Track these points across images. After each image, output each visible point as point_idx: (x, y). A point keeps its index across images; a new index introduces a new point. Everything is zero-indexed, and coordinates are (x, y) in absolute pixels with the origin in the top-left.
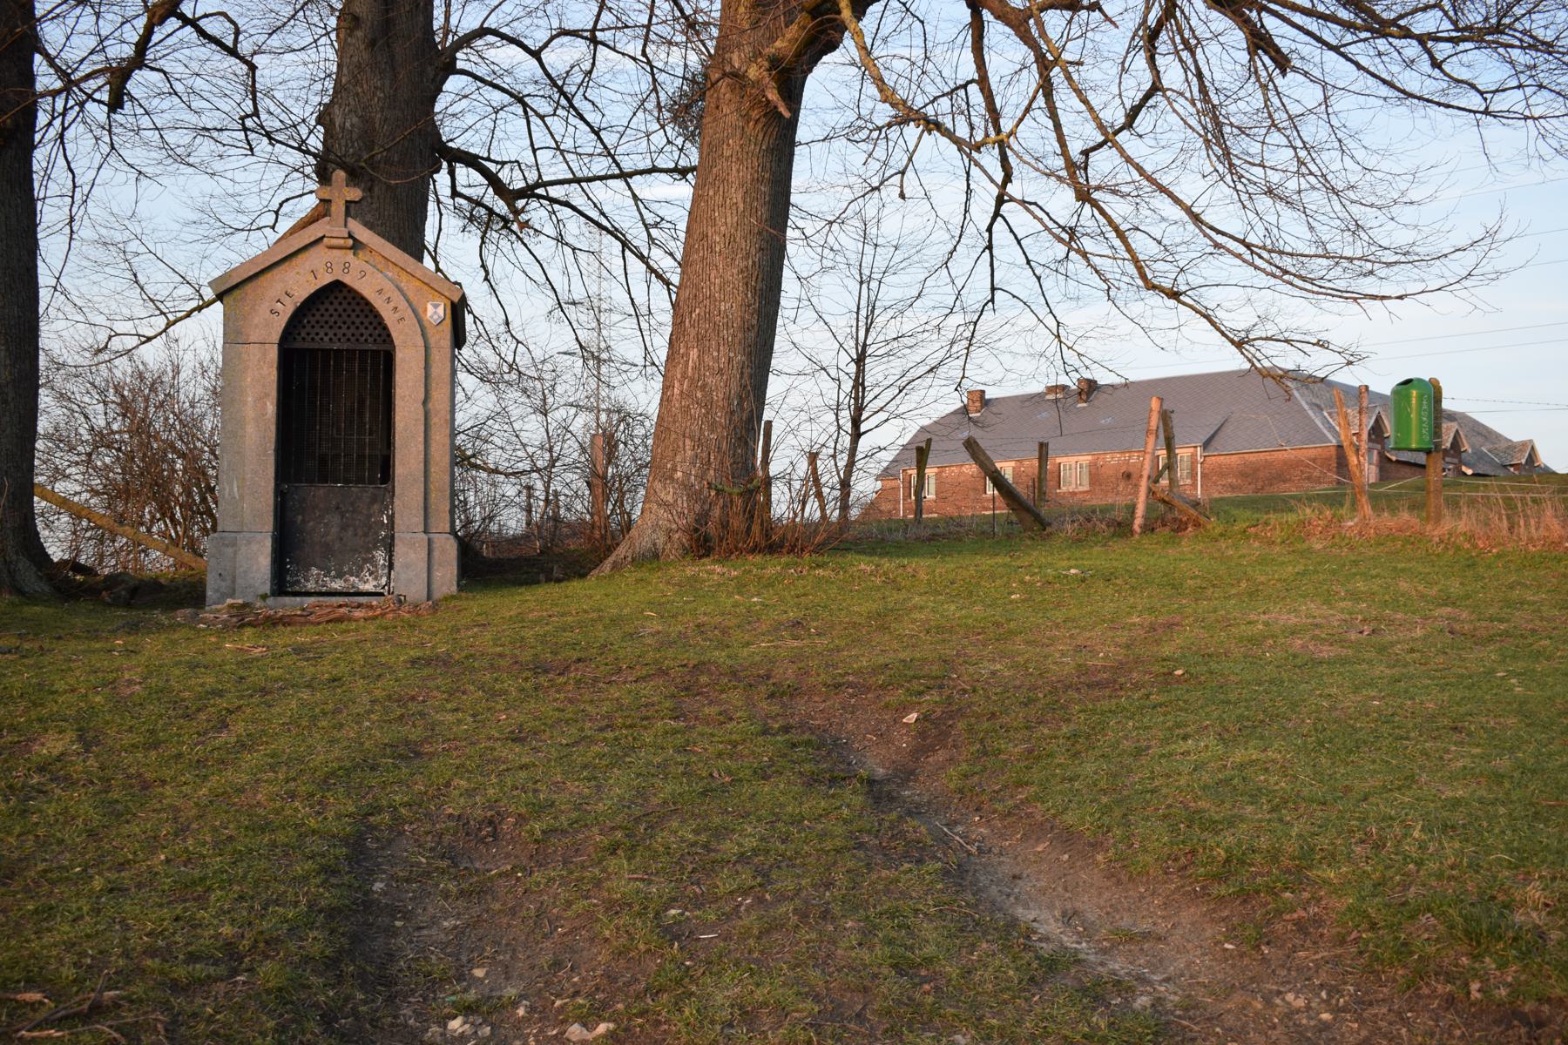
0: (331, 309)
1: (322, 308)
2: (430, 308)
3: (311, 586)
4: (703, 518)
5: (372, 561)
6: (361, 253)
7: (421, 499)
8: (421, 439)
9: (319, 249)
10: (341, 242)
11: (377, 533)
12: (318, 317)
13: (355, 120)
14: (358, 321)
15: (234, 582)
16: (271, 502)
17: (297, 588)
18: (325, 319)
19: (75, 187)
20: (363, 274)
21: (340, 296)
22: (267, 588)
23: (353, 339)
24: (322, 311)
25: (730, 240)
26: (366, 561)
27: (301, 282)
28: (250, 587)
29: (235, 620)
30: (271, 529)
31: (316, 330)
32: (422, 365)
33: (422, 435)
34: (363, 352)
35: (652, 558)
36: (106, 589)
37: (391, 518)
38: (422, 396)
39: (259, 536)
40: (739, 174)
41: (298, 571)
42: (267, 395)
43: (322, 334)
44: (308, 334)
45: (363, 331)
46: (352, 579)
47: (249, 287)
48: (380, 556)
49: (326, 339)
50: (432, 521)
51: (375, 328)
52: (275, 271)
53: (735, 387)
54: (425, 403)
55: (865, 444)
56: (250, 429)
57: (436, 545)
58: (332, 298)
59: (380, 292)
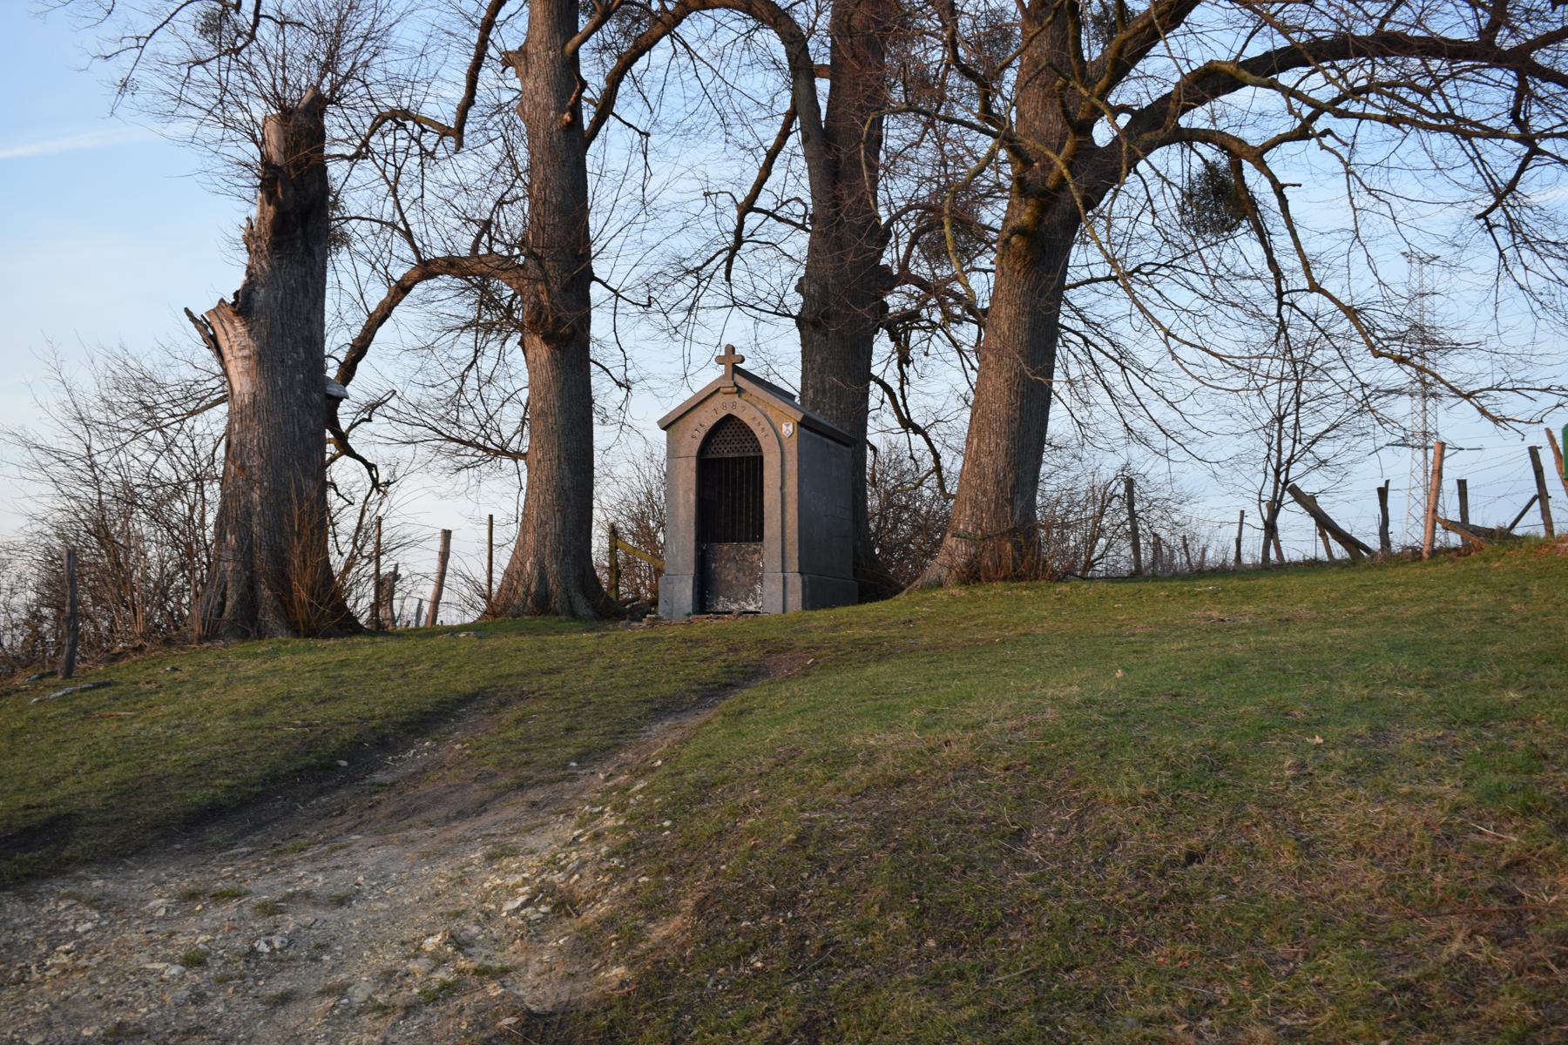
3: (720, 608)
5: (754, 591)
6: (743, 396)
8: (779, 512)
9: (719, 395)
13: (816, 287)
20: (744, 408)
22: (690, 609)
26: (750, 591)
27: (707, 418)
30: (692, 571)
38: (779, 484)
47: (680, 423)
48: (758, 587)
50: (788, 564)
52: (695, 412)
53: (1001, 463)
54: (782, 488)
56: (681, 510)
59: (754, 419)
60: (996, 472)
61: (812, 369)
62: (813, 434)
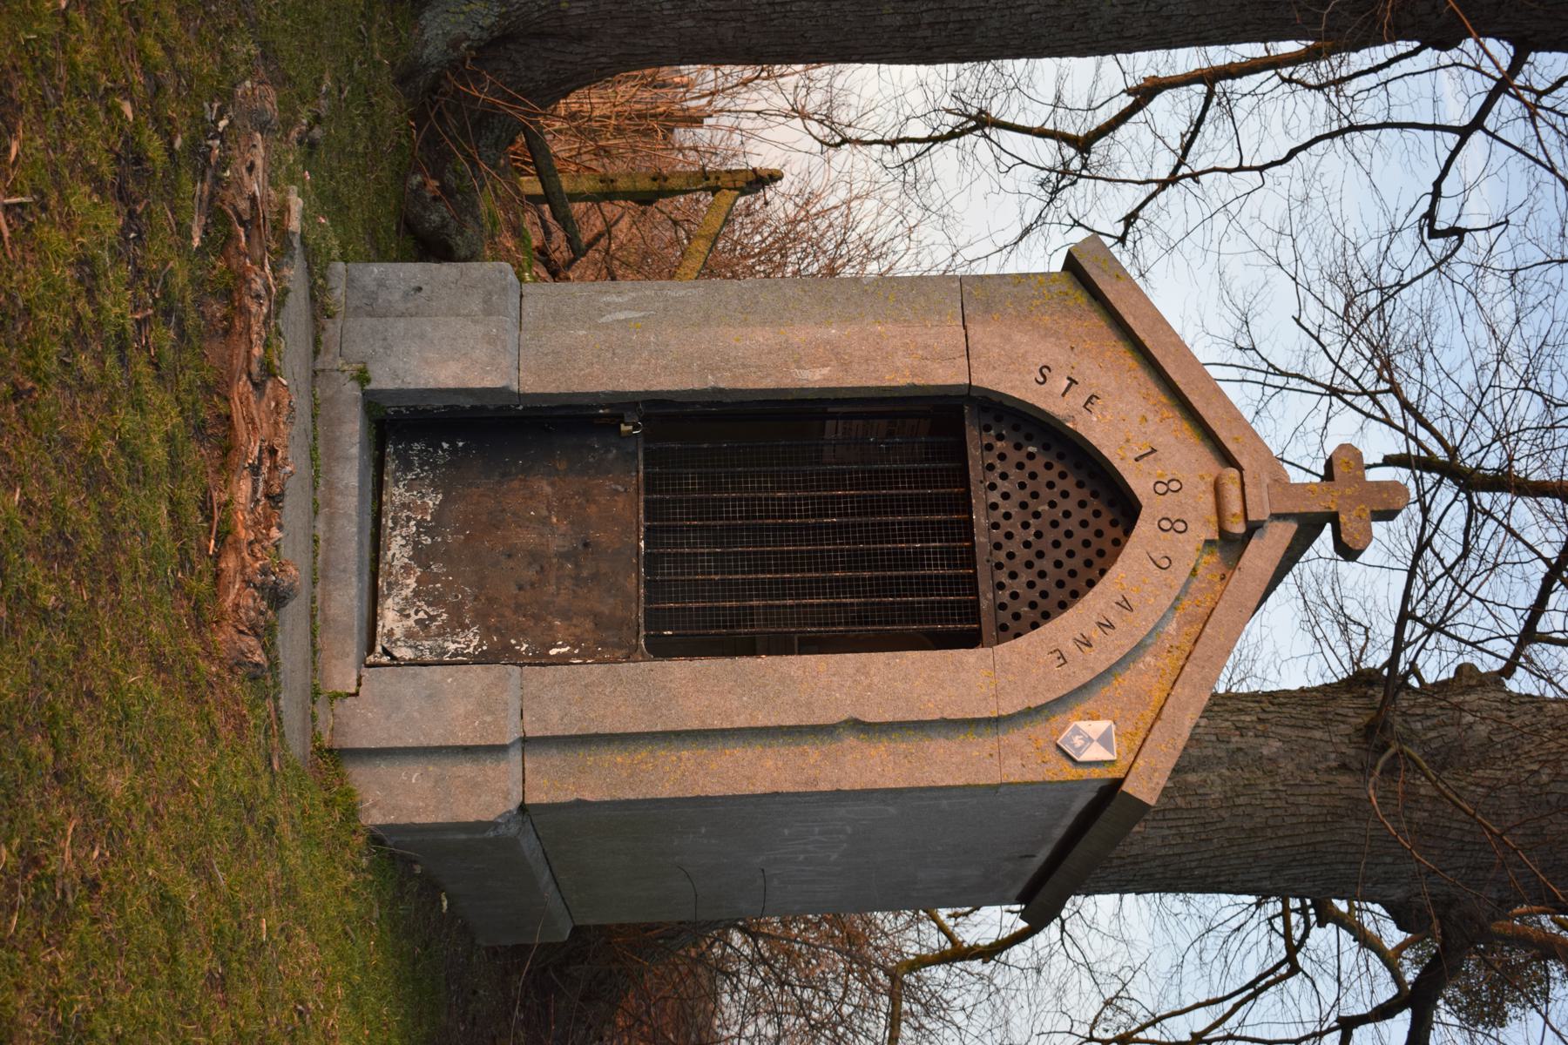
0: (1070, 504)
1: (1068, 484)
2: (1102, 726)
3: (396, 494)
5: (457, 624)
6: (1213, 559)
7: (606, 728)
8: (762, 720)
10: (1235, 507)
11: (522, 633)
12: (1045, 476)
13: (1482, 730)
14: (1046, 564)
15: (402, 315)
16: (592, 387)
17: (391, 466)
18: (1045, 493)
19: (1261, 169)
20: (1164, 564)
21: (1103, 523)
22: (382, 380)
23: (1001, 556)
24: (1061, 485)
26: (456, 612)
28: (388, 347)
29: (243, 205)
31: (1014, 473)
32: (953, 713)
33: (773, 721)
34: (972, 583)
36: (443, 188)
37: (563, 660)
38: (870, 718)
39: (507, 361)
41: (434, 467)
42: (845, 366)
43: (1003, 486)
44: (1002, 457)
45: (1024, 577)
46: (412, 582)
47: (1096, 322)
48: (470, 640)
49: (995, 497)
50: (555, 759)
51: (1033, 605)
52: (1140, 377)
54: (858, 726)
57: (490, 769)
58: (1095, 504)
59: (1125, 604)
61: (1241, 730)
62: (1068, 821)
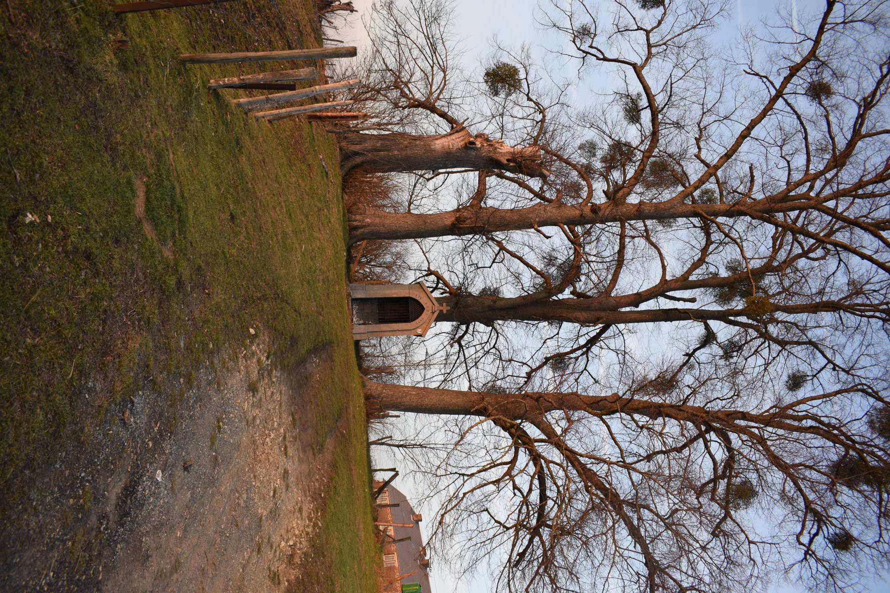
4: (374, 397)
25: (443, 400)
35: (364, 386)
40: (460, 401)
48: (361, 322)
55: (396, 449)
56: (389, 292)
60: (404, 402)
